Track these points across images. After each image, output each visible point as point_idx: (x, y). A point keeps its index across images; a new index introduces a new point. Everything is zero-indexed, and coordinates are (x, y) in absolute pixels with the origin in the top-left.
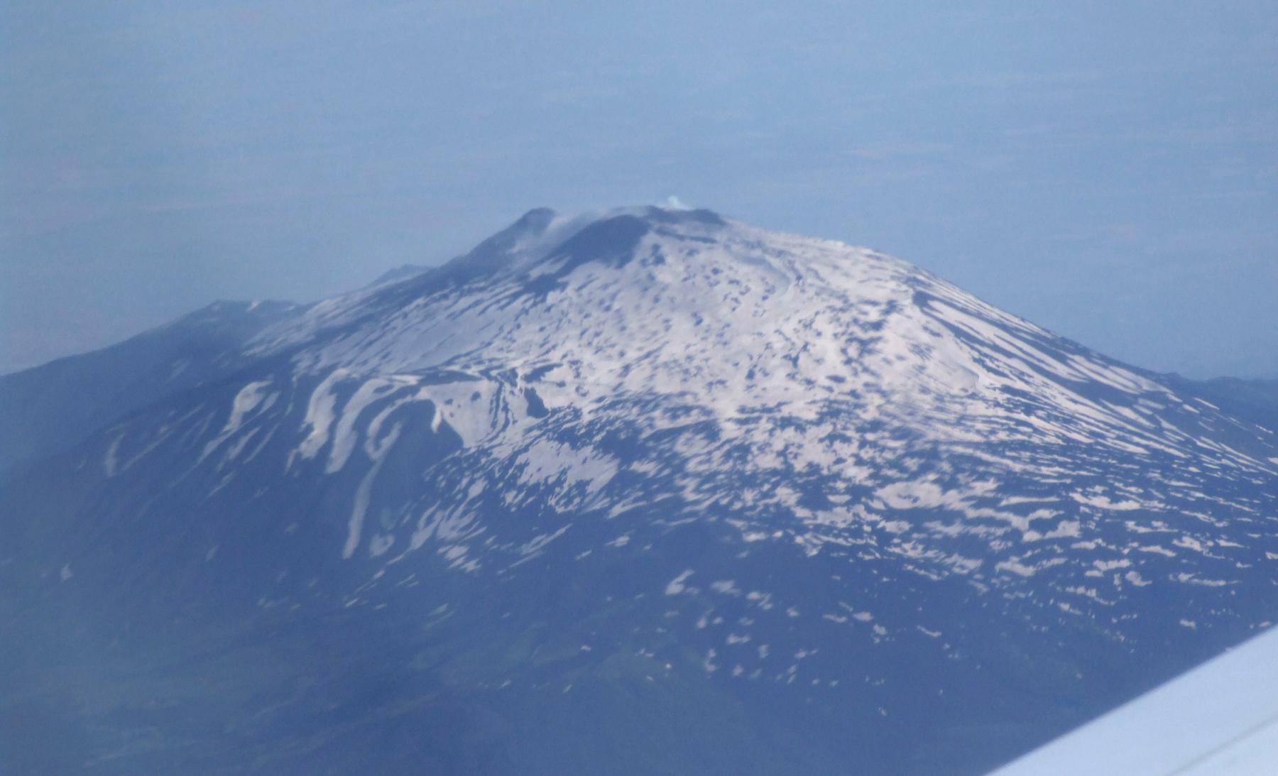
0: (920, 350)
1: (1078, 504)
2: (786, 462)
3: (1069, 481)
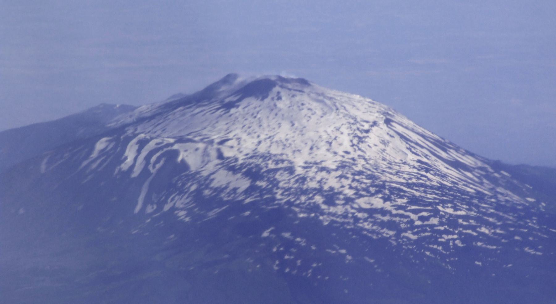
0: (384, 142)
1: (439, 211)
2: (320, 186)
3: (437, 201)
